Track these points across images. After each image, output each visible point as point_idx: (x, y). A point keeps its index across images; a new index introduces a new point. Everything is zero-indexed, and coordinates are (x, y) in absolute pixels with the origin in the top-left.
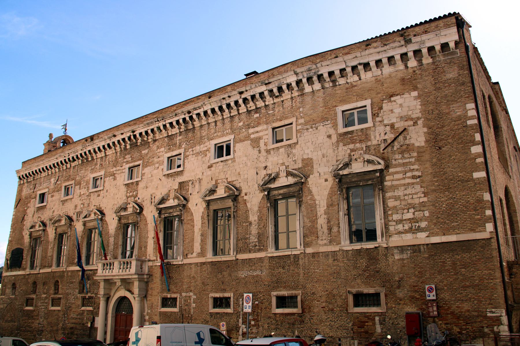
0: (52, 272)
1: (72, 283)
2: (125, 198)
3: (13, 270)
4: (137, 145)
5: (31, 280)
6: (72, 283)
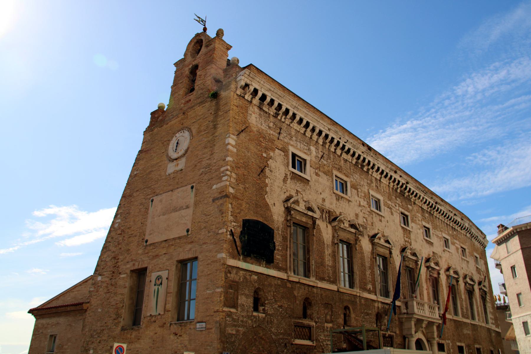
1: (368, 314)
2: (403, 240)
3: (248, 259)
4: (404, 196)
5: (300, 294)
6: (368, 314)
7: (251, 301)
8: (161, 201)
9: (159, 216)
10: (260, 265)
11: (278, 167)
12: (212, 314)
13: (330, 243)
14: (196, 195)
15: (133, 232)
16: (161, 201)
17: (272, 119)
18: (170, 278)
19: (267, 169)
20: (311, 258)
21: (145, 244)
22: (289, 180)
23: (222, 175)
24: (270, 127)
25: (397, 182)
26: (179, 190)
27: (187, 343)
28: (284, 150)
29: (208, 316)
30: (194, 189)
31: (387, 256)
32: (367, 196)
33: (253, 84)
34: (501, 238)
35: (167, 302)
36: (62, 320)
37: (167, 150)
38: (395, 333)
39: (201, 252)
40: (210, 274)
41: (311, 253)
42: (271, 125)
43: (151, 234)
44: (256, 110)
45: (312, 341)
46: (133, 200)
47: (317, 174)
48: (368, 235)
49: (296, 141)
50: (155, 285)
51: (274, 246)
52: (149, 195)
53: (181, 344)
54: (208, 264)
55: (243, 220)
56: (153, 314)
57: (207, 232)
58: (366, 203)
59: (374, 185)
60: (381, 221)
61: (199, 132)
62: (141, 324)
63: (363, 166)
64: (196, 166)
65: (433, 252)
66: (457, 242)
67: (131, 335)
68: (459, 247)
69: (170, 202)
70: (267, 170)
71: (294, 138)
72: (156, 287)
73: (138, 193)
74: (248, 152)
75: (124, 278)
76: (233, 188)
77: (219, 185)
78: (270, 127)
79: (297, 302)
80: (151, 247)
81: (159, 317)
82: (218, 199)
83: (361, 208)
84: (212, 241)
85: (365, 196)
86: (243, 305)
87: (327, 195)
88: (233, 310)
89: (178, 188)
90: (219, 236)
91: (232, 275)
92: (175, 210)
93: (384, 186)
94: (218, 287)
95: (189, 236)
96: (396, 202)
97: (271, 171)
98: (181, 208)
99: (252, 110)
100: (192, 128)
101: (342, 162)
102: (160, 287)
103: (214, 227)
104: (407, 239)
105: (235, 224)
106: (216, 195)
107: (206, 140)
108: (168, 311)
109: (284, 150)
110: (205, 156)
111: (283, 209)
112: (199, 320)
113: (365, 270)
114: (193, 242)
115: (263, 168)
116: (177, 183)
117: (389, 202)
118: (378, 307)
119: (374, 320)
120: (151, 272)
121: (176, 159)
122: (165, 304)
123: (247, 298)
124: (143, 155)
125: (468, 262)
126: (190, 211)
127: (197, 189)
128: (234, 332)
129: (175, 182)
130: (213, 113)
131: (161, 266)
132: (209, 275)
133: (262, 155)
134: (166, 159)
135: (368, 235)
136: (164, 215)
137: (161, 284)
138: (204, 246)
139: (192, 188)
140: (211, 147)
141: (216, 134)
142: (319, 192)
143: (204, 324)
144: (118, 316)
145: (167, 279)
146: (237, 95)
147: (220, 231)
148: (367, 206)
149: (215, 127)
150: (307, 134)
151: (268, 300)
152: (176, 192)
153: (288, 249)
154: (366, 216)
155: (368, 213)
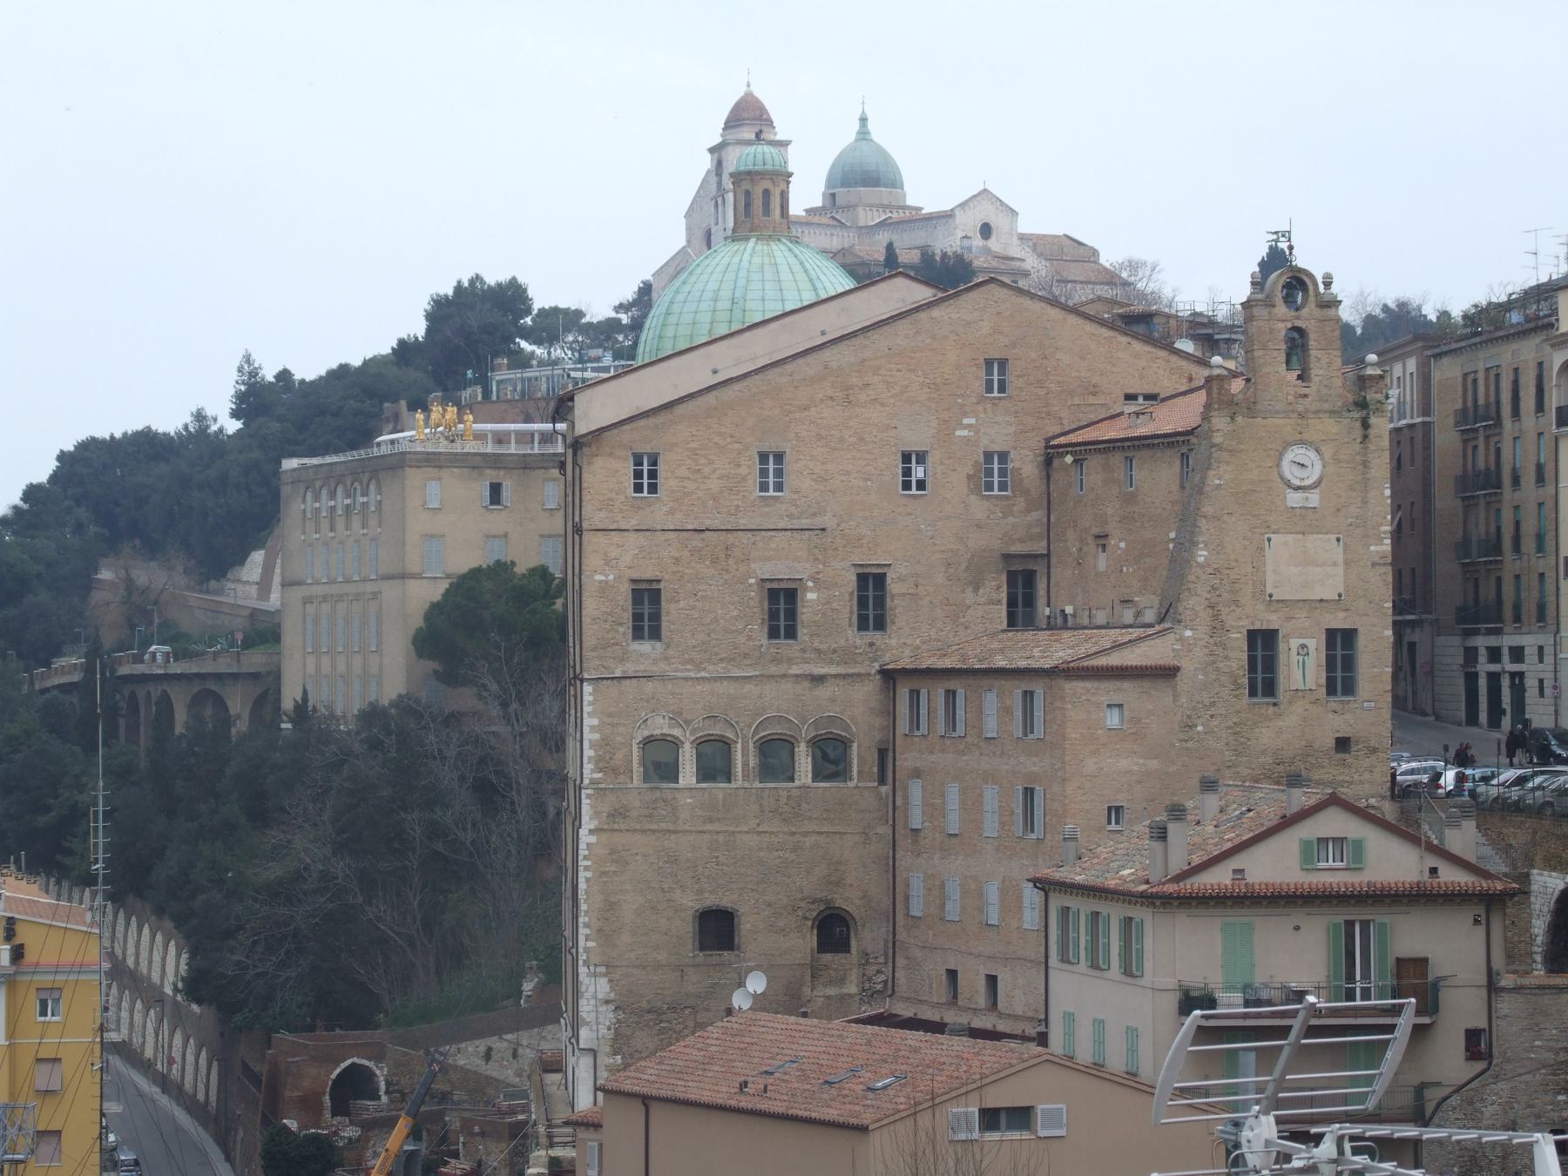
14: (1345, 551)
36: (1127, 685)
37: (1278, 465)
61: (1337, 460)
77: (1379, 548)
100: (1323, 449)
106: (1376, 559)
126: (1340, 570)
144: (1238, 687)
149: (1365, 464)
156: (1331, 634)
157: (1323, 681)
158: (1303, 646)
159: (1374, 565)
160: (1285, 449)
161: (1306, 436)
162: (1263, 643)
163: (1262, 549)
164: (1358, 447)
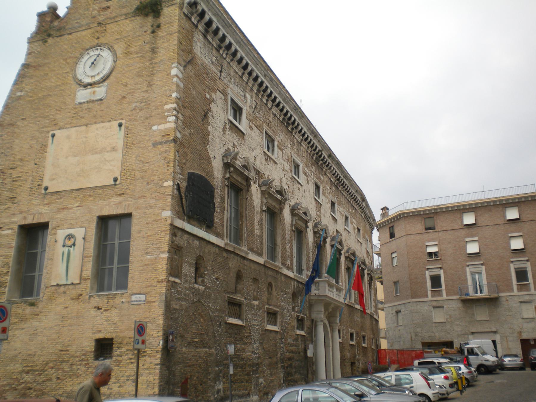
0: (264, 266)
3: (191, 221)
4: (318, 164)
7: (193, 270)
8: (68, 137)
9: (67, 157)
10: (201, 229)
11: (220, 114)
12: (154, 284)
13: (259, 209)
14: (126, 134)
15: (20, 175)
16: (68, 137)
17: (214, 52)
18: (87, 238)
19: (210, 113)
20: (244, 225)
21: (43, 192)
22: (228, 130)
23: (166, 114)
24: (212, 62)
25: (315, 147)
26: (98, 125)
27: (116, 319)
28: (224, 93)
29: (149, 286)
30: (123, 127)
31: (303, 230)
32: (289, 159)
33: (202, 4)
34: (385, 222)
35: (84, 268)
37: (74, 70)
38: (306, 315)
39: (137, 208)
40: (151, 235)
41: (244, 220)
42: (214, 59)
43: (53, 179)
44: (201, 37)
45: (242, 320)
46: (16, 130)
47: (251, 128)
48: (289, 204)
49: (234, 84)
50: (64, 246)
51: (214, 207)
52: (46, 127)
53: (107, 321)
54: (147, 223)
55: (189, 173)
56: (60, 283)
57: (145, 184)
58: (288, 167)
59: (295, 147)
60: (299, 189)
61: (127, 53)
62: (41, 295)
63: (288, 124)
64: (124, 97)
65: (337, 230)
66: (355, 222)
67: (24, 310)
68: (356, 227)
69: (84, 139)
70: (209, 115)
71: (233, 80)
72: (66, 249)
73: (25, 123)
74: (194, 89)
75: (7, 235)
76: (180, 132)
77: (162, 127)
78: (212, 62)
79: (231, 275)
80: (55, 197)
81: (71, 287)
82: (161, 143)
83: (284, 173)
84: (154, 195)
85: (288, 160)
86: (187, 275)
87: (257, 153)
88: (177, 280)
89: (95, 123)
90: (163, 190)
91: (177, 238)
92: (94, 151)
93: (304, 150)
94: (163, 252)
95: (117, 186)
96: (311, 170)
97: (213, 117)
98: (103, 150)
99: (197, 36)
100: (116, 47)
101: (272, 116)
102: (72, 249)
103: (156, 177)
104: (318, 213)
105: (181, 176)
106: (159, 139)
107: (138, 66)
108: (86, 279)
109: (224, 93)
110: (139, 86)
111: (222, 164)
112: (135, 291)
113: (285, 243)
114: (123, 194)
115: (206, 111)
116: (95, 116)
117: (306, 169)
118: (294, 286)
119: (290, 300)
120: (56, 228)
121: (91, 85)
122: (82, 271)
123: (190, 267)
124: (31, 71)
125: (361, 244)
126: (119, 155)
127: (127, 128)
128: (178, 307)
129: (89, 114)
130: (149, 32)
131: (72, 222)
132: (148, 236)
133: (205, 95)
134: (72, 82)
135: (289, 204)
136: (75, 156)
137: (74, 245)
138: (142, 201)
139: (120, 125)
140: (149, 76)
141: (156, 61)
142: (251, 150)
143: (143, 297)
145: (84, 239)
146: (184, 13)
147: (165, 184)
148: (289, 171)
149: (154, 51)
150: (244, 78)
151: (207, 271)
152: (94, 127)
153: (226, 212)
154: (289, 182)
155: (290, 179)
156: (104, 221)
157: (88, 272)
158: (70, 237)
159: (155, 144)
160: (82, 55)
161: (103, 40)
162: (33, 234)
163: (46, 146)
164: (148, 37)
